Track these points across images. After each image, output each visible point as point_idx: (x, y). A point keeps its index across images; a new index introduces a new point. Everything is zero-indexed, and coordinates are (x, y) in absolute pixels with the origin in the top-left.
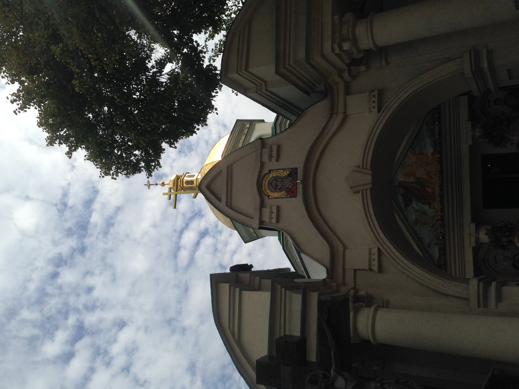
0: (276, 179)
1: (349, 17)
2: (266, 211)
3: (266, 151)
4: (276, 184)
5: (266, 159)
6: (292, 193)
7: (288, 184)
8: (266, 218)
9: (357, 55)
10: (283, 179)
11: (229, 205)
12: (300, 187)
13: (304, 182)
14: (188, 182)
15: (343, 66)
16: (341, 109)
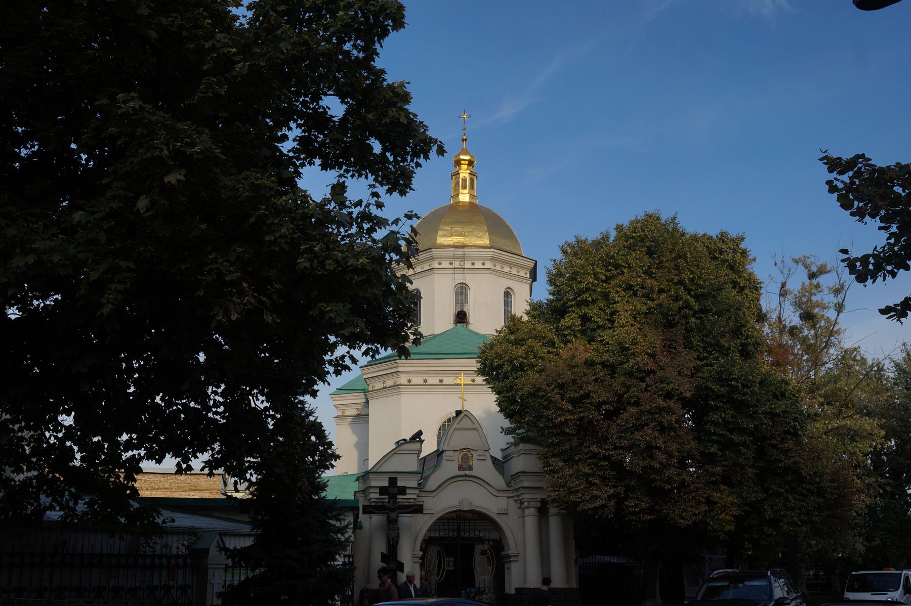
0: (468, 458)
1: (539, 505)
2: (451, 453)
3: (483, 453)
4: (465, 458)
5: (479, 453)
6: (461, 468)
7: (465, 466)
8: (448, 453)
9: (523, 506)
10: (468, 462)
11: (456, 429)
12: (463, 473)
13: (466, 476)
14: (464, 180)
15: (521, 497)
16: (500, 495)
